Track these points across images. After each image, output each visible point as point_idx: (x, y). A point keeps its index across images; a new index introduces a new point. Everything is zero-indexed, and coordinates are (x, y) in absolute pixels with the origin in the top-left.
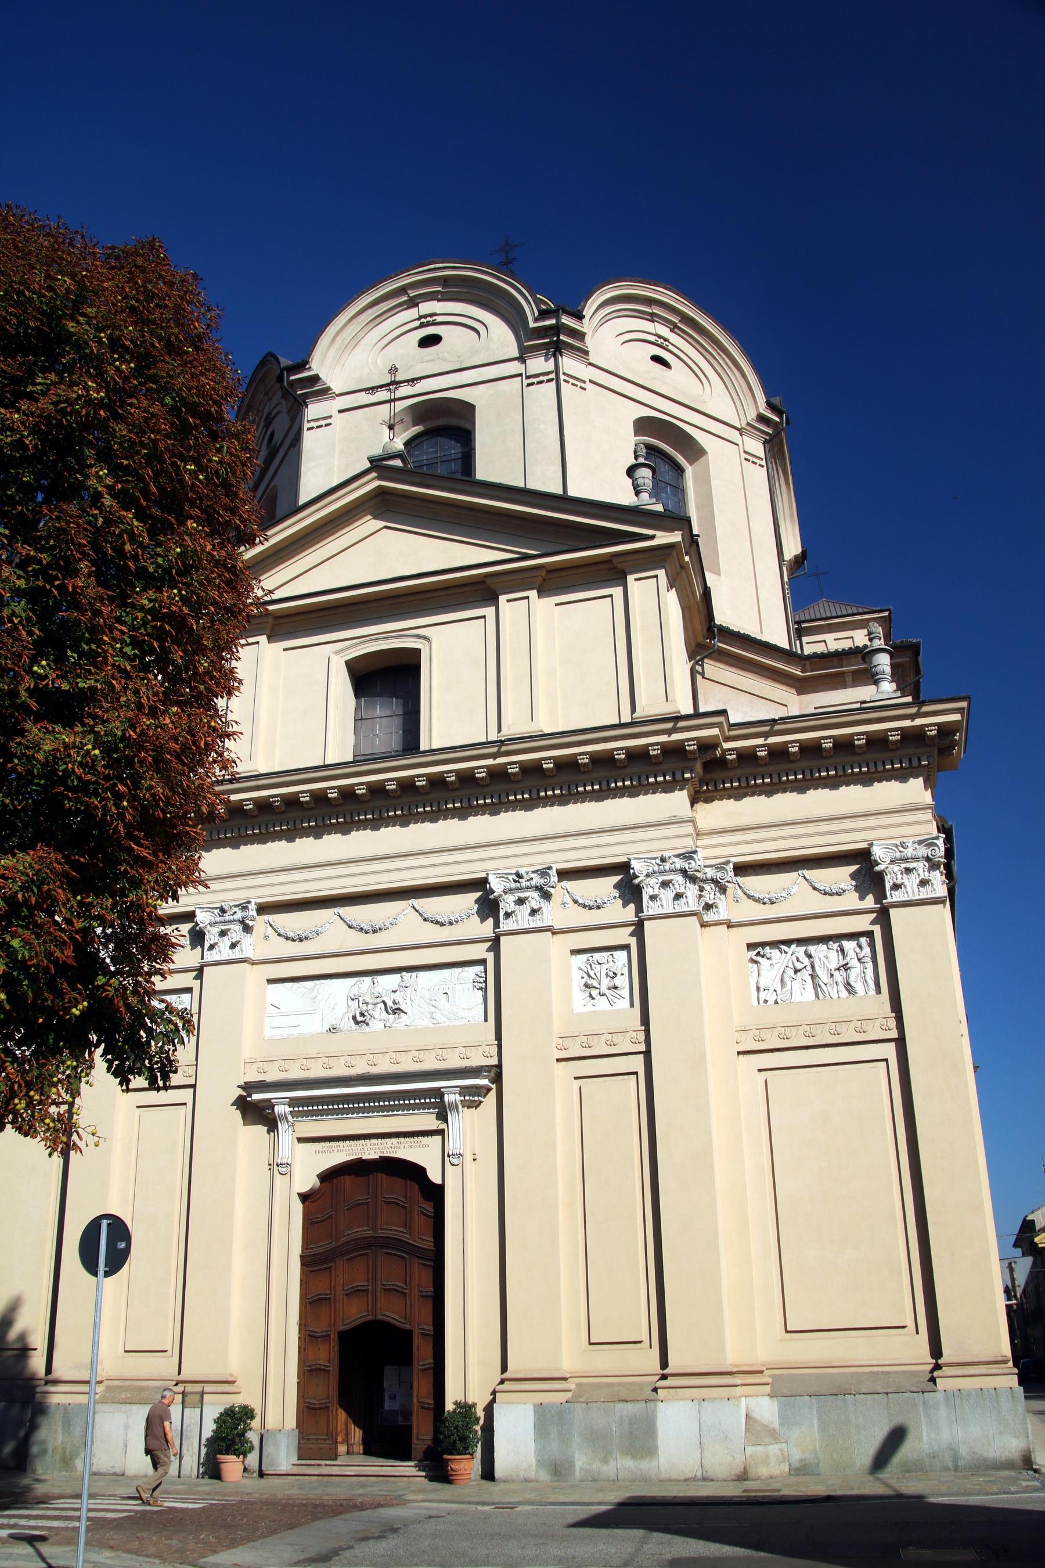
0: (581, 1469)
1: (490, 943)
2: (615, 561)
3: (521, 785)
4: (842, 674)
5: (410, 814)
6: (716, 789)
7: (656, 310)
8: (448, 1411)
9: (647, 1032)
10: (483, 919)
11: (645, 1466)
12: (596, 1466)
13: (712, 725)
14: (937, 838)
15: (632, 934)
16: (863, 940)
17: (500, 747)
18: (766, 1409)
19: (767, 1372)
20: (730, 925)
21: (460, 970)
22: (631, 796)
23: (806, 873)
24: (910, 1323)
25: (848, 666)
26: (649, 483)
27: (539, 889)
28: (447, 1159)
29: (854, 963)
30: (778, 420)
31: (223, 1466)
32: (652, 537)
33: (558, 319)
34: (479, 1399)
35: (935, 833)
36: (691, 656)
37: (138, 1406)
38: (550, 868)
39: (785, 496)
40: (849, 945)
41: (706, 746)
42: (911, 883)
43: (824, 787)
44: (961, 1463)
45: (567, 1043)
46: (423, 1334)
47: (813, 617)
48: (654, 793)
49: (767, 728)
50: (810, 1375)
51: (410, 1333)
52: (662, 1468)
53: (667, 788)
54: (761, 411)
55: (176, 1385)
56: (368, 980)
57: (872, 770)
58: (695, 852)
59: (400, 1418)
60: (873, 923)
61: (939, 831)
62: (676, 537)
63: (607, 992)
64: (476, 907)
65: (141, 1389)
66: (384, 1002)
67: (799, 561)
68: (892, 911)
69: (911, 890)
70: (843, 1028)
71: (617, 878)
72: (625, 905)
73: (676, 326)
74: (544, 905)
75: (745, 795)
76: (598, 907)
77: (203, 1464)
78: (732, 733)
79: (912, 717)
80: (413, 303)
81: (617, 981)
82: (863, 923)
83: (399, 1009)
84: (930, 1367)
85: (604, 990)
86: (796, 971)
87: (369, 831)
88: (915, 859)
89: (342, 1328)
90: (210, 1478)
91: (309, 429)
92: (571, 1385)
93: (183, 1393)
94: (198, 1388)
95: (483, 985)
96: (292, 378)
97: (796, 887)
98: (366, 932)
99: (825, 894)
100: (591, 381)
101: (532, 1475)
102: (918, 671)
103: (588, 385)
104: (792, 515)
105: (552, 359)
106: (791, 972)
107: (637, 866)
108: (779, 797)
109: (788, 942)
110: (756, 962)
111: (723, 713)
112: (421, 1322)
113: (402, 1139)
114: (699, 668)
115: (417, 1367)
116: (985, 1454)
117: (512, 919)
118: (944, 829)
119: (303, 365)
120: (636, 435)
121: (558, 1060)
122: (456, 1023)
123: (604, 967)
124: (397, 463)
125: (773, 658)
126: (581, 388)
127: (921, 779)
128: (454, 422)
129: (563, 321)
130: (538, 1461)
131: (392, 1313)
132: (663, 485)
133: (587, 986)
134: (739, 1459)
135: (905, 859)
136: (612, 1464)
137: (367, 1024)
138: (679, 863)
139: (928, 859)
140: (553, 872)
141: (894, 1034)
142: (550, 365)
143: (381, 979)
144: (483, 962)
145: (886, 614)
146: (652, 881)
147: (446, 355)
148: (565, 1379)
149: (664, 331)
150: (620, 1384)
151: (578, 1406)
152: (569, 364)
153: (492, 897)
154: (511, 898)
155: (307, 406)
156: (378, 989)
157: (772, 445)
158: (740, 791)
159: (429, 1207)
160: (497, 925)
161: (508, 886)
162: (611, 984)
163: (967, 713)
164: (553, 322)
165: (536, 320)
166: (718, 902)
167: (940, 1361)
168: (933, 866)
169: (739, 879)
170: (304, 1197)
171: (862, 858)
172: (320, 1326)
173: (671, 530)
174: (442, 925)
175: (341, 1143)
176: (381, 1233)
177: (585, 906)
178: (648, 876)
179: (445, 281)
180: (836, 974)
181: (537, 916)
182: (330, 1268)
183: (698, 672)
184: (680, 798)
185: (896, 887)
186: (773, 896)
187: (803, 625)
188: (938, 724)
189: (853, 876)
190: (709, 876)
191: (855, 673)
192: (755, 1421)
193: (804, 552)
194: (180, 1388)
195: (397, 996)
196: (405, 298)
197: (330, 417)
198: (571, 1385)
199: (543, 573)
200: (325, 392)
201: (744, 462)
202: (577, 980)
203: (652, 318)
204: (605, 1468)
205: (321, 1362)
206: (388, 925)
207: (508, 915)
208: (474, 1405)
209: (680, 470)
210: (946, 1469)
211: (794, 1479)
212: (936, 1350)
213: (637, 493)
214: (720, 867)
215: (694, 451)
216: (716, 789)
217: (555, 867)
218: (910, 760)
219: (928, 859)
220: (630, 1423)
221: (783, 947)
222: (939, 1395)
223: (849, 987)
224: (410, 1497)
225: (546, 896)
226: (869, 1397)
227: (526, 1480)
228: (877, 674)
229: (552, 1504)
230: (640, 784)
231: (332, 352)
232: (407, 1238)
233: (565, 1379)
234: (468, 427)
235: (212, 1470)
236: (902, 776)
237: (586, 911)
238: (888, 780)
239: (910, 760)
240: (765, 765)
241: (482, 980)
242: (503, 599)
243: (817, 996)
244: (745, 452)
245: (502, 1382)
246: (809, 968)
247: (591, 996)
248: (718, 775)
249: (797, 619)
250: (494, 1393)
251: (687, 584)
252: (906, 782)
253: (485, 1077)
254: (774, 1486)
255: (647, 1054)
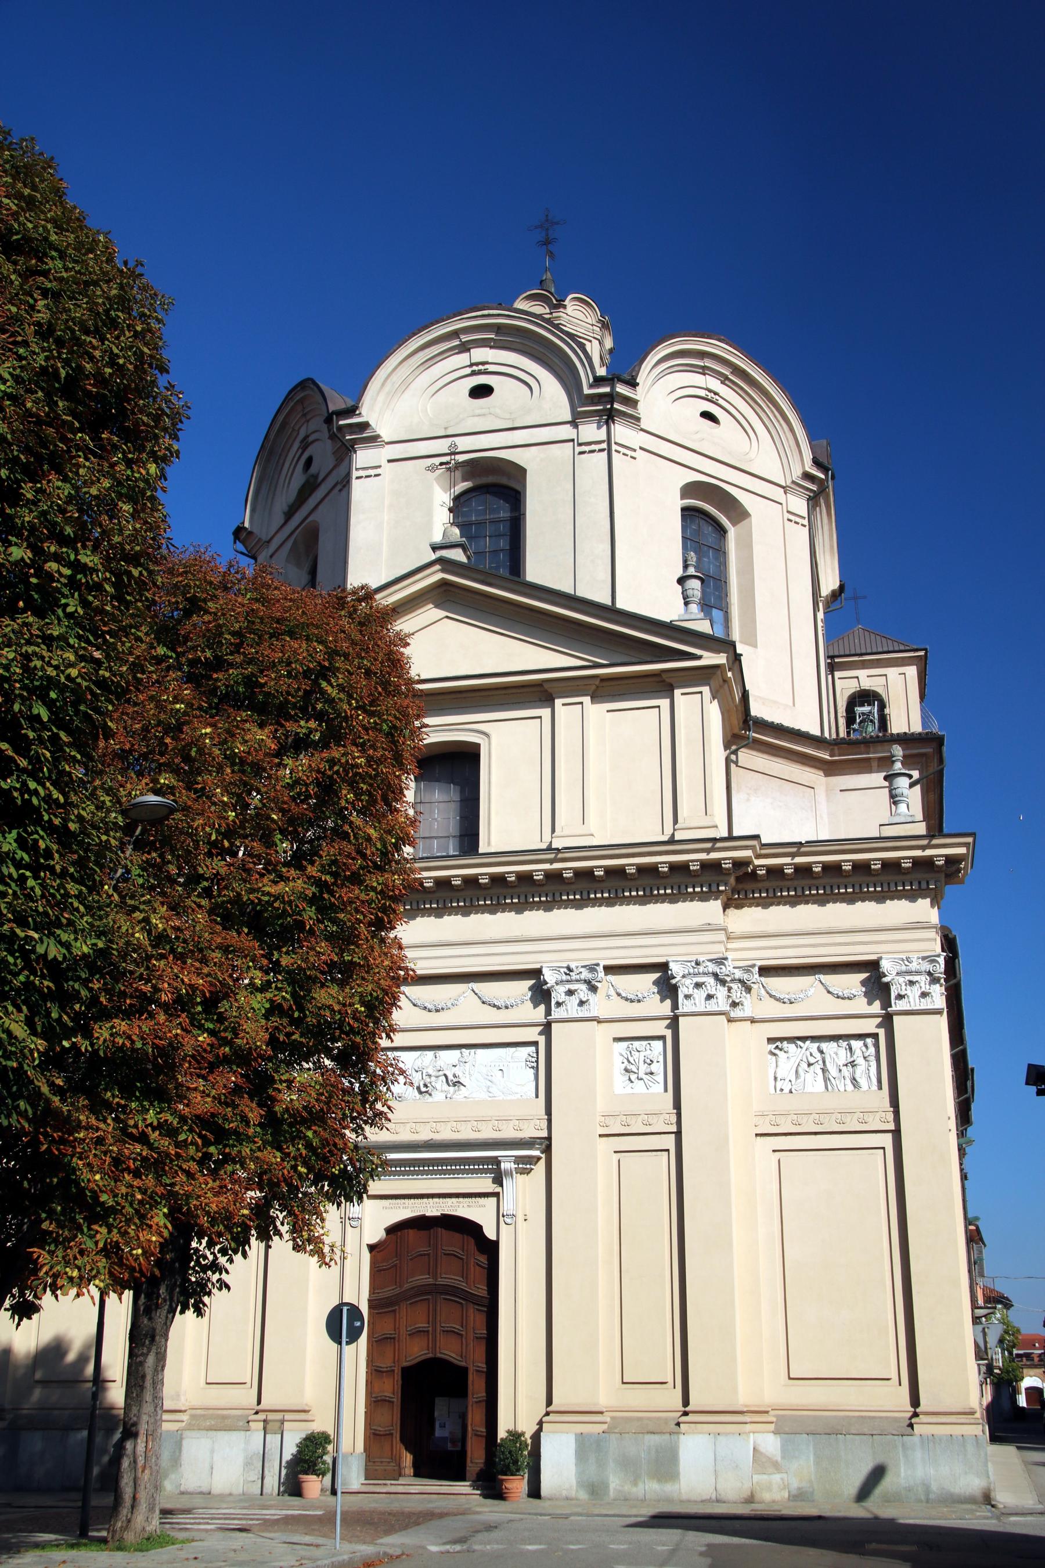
0: (615, 1489)
1: (541, 1028)
2: (664, 676)
3: (573, 887)
4: (869, 759)
5: (472, 905)
6: (746, 898)
7: (708, 363)
8: (502, 1439)
9: (679, 1115)
10: (535, 1007)
11: (669, 1488)
12: (627, 1488)
13: (746, 848)
14: (939, 956)
15: (667, 1027)
16: (870, 1041)
17: (557, 854)
18: (770, 1444)
19: (772, 1413)
20: (753, 1021)
21: (513, 1049)
22: (671, 902)
23: (822, 977)
24: (894, 1376)
25: (874, 753)
26: (698, 594)
27: (588, 982)
28: (501, 1219)
29: (860, 1061)
30: (823, 476)
31: (305, 1485)
32: (700, 657)
33: (613, 388)
34: (527, 1428)
35: (938, 949)
36: (726, 747)
37: (223, 1432)
38: (598, 965)
39: (826, 528)
40: (857, 1044)
41: (739, 864)
42: (914, 993)
43: (843, 901)
44: (932, 1496)
45: (610, 1121)
46: (478, 1371)
47: (847, 653)
48: (692, 900)
49: (795, 850)
50: (808, 1416)
51: (464, 1371)
52: (683, 1491)
53: (703, 897)
54: (807, 469)
55: (257, 1413)
56: (430, 1054)
57: (886, 889)
58: (726, 959)
59: (449, 1445)
60: (878, 1026)
61: (943, 951)
62: (721, 659)
63: (644, 1077)
64: (530, 994)
65: (224, 1417)
66: (445, 1075)
67: (835, 595)
68: (895, 1018)
69: (913, 1001)
70: (848, 1118)
71: (656, 976)
72: (662, 1001)
73: (727, 378)
74: (592, 997)
75: (772, 904)
76: (639, 1001)
77: (284, 1484)
78: (764, 852)
79: (923, 848)
80: (464, 348)
81: (654, 1067)
82: (870, 1026)
83: (459, 1082)
84: (910, 1414)
85: (641, 1075)
86: (809, 1065)
87: (432, 918)
88: (918, 973)
89: (405, 1364)
90: (290, 1495)
91: (358, 478)
92: (606, 1418)
93: (264, 1421)
94: (279, 1416)
95: (535, 1065)
96: (341, 423)
97: (812, 990)
98: (430, 1011)
99: (838, 997)
100: (641, 448)
101: (573, 1494)
102: (941, 761)
103: (639, 454)
104: (832, 547)
105: (605, 427)
106: (804, 1065)
107: (675, 968)
108: (801, 908)
109: (803, 1039)
110: (775, 1055)
111: (757, 837)
112: (476, 1360)
113: (461, 1200)
114: (733, 757)
115: (471, 1400)
116: (952, 1490)
117: (563, 1008)
118: (949, 944)
119: (352, 411)
120: (683, 497)
121: (600, 1136)
122: (509, 1098)
123: (642, 1054)
124: (458, 555)
125: (804, 745)
126: (632, 457)
127: (928, 900)
128: (504, 481)
129: (618, 390)
130: (578, 1483)
131: (450, 1351)
132: (706, 548)
133: (626, 1070)
134: (747, 1486)
135: (909, 973)
136: (641, 1485)
137: (430, 1095)
138: (712, 967)
139: (929, 974)
140: (600, 969)
141: (892, 1126)
142: (602, 434)
143: (442, 1054)
144: (535, 1044)
145: (922, 653)
146: (688, 981)
147: (498, 411)
148: (601, 1413)
149: (714, 384)
150: (649, 1419)
151: (613, 1436)
152: (621, 431)
153: (545, 987)
154: (562, 989)
155: (355, 452)
156: (440, 1063)
157: (813, 501)
158: (767, 900)
159: (483, 1259)
160: (548, 1012)
161: (560, 978)
162: (648, 1071)
163: (973, 848)
164: (607, 390)
165: (591, 386)
166: (743, 999)
167: (918, 1410)
168: (934, 980)
169: (763, 979)
170: (372, 1248)
171: (872, 967)
172: (386, 1363)
173: (718, 652)
174: (499, 1008)
175: (406, 1201)
176: (441, 1281)
177: (627, 999)
178: (684, 976)
179: (499, 329)
180: (844, 1069)
181: (585, 1007)
182: (394, 1311)
183: (733, 761)
184: (715, 906)
185: (900, 997)
186: (792, 996)
187: (836, 660)
188: (946, 856)
189: (863, 983)
190: (737, 977)
191: (880, 759)
192: (761, 1453)
193: (842, 587)
194: (262, 1416)
195: (457, 1071)
196: (456, 342)
197: (380, 467)
198: (606, 1418)
199: (597, 682)
200: (375, 439)
201: (787, 522)
202: (619, 1066)
203: (704, 371)
204: (634, 1489)
205: (386, 1394)
206: (449, 1005)
207: (559, 1004)
208: (523, 1434)
209: (722, 531)
210: (920, 1501)
211: (791, 1504)
212: (915, 1401)
213: (686, 604)
214: (747, 970)
215: (738, 512)
216: (746, 898)
217: (602, 963)
218: (920, 883)
219: (929, 974)
220: (657, 1451)
221: (799, 1043)
222: (916, 1439)
223: (854, 1080)
224: (478, 1509)
225: (593, 989)
226: (857, 1437)
227: (567, 1499)
228: (896, 796)
229: (598, 1515)
230: (680, 893)
231: (381, 398)
232: (463, 1285)
233: (601, 1413)
234: (518, 487)
235: (293, 1488)
236: (912, 897)
237: (628, 1003)
238: (899, 898)
239: (920, 883)
240: (791, 879)
241: (534, 1060)
242: (558, 702)
243: (827, 1088)
244: (788, 512)
245: (547, 1414)
246: (821, 1062)
247: (630, 1079)
248: (749, 886)
249: (831, 654)
250: (540, 1423)
251: (728, 693)
252: (914, 902)
253: (537, 1149)
254: (776, 1507)
255: (678, 1134)
